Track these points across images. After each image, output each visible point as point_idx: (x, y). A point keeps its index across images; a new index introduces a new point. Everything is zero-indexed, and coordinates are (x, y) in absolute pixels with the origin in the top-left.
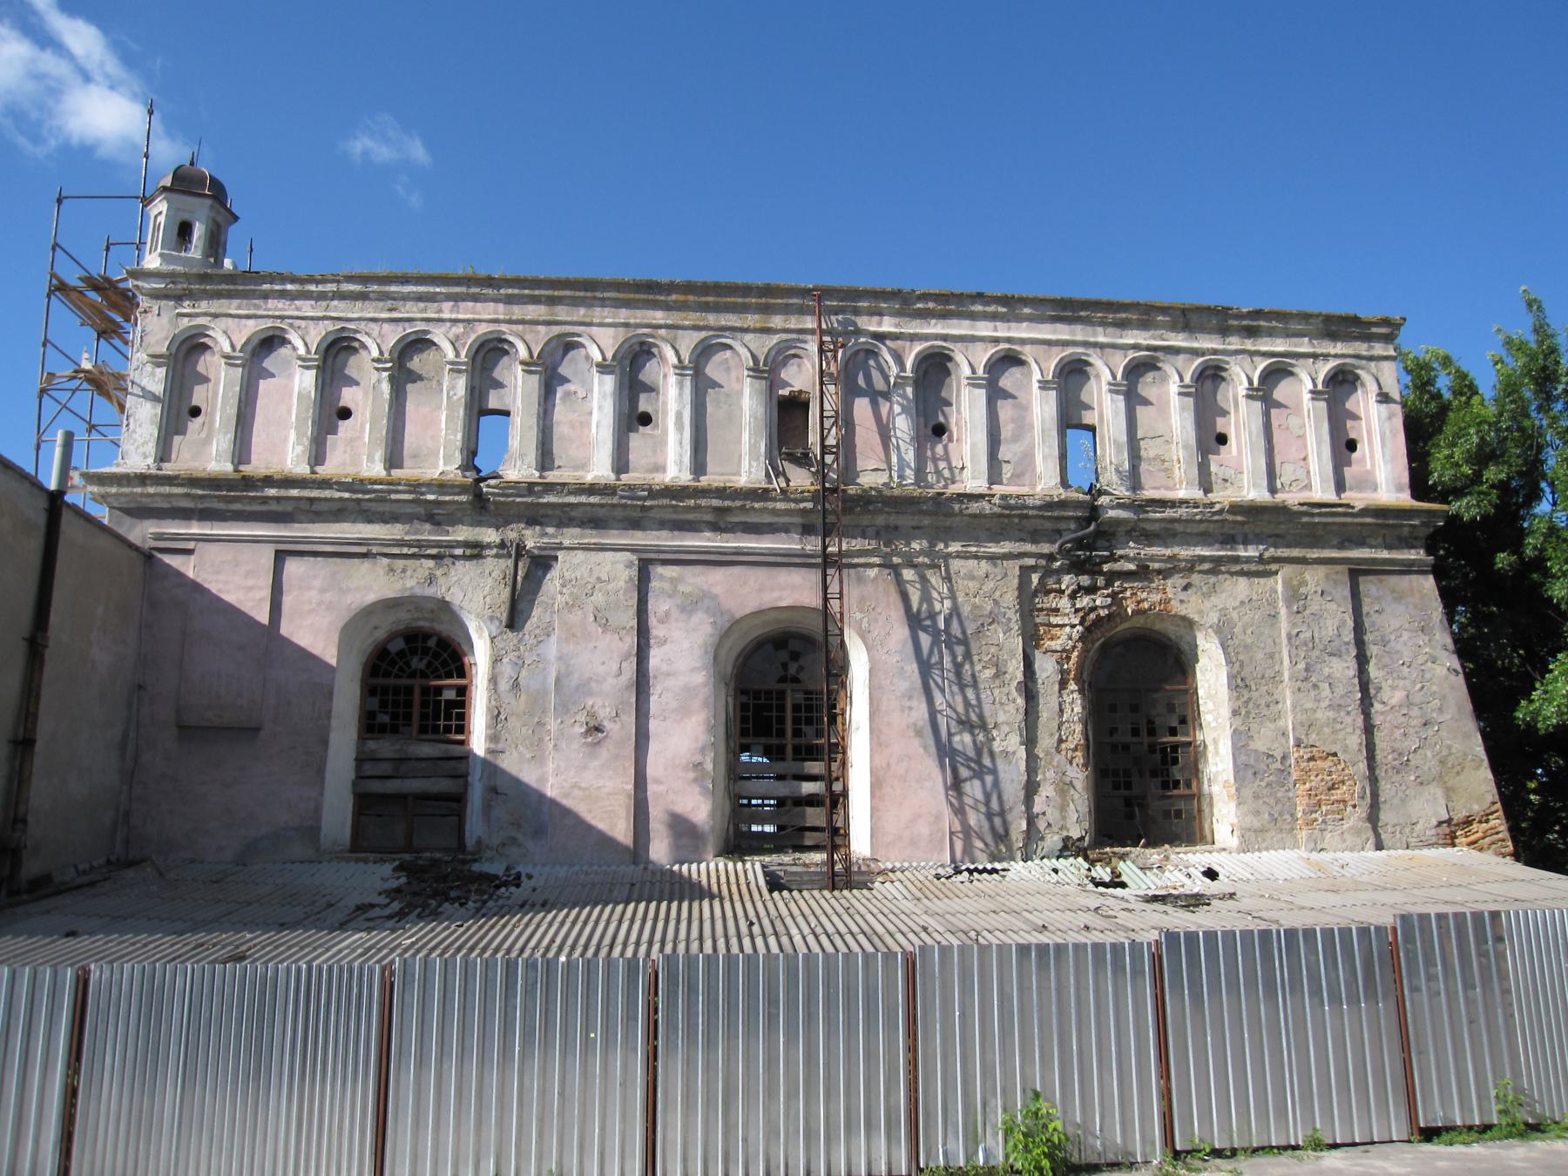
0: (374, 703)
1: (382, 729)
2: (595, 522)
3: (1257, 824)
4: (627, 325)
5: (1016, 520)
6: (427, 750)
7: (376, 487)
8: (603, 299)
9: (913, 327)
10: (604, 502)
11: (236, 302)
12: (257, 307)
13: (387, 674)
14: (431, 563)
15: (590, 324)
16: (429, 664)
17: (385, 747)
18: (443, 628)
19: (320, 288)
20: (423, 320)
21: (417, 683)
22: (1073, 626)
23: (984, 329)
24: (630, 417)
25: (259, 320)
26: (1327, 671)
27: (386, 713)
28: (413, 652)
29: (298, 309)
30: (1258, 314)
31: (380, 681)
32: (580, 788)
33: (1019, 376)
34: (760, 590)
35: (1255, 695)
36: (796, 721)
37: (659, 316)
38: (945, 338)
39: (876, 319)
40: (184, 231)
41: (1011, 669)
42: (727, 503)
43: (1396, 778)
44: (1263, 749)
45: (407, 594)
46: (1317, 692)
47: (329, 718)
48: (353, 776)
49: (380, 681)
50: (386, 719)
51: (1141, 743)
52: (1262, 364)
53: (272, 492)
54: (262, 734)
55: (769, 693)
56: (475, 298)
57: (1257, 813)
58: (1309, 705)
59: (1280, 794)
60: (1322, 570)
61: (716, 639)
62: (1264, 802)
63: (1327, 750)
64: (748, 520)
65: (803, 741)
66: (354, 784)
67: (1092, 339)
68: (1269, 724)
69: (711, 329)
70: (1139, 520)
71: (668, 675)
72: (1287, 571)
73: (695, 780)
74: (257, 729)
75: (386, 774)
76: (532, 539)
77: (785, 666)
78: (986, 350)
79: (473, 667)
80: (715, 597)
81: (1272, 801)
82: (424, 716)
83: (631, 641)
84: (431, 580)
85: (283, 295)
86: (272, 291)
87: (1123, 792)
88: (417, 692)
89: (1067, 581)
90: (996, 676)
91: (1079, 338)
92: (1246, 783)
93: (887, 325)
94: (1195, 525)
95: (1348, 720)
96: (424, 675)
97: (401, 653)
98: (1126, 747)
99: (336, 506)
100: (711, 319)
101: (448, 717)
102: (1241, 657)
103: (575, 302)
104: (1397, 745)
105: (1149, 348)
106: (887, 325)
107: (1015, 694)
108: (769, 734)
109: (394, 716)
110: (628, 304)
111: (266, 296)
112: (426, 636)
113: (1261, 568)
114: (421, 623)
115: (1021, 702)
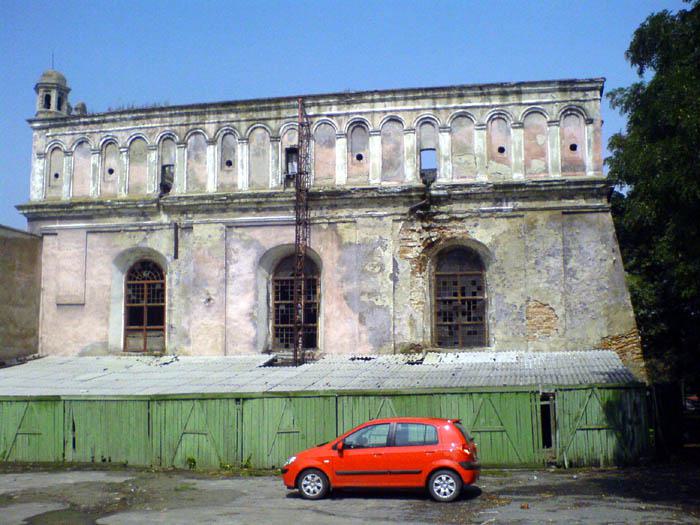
0: (131, 292)
2: (209, 211)
3: (506, 338)
9: (345, 110)
11: (68, 128)
13: (135, 279)
14: (144, 233)
18: (154, 259)
23: (379, 107)
26: (547, 264)
28: (144, 269)
30: (520, 84)
31: (132, 282)
38: (361, 113)
40: (48, 99)
42: (261, 199)
43: (581, 316)
44: (510, 302)
49: (132, 282)
51: (456, 300)
52: (524, 109)
53: (83, 208)
54: (86, 306)
55: (287, 281)
57: (506, 333)
58: (536, 281)
60: (547, 213)
63: (544, 302)
74: (84, 305)
80: (258, 241)
81: (514, 327)
82: (149, 296)
84: (145, 239)
87: (448, 323)
88: (146, 288)
89: (418, 226)
93: (334, 110)
95: (556, 288)
98: (450, 301)
100: (255, 115)
104: (584, 300)
105: (462, 108)
106: (334, 110)
107: (389, 280)
108: (287, 299)
109: (138, 296)
113: (515, 214)
115: (392, 283)
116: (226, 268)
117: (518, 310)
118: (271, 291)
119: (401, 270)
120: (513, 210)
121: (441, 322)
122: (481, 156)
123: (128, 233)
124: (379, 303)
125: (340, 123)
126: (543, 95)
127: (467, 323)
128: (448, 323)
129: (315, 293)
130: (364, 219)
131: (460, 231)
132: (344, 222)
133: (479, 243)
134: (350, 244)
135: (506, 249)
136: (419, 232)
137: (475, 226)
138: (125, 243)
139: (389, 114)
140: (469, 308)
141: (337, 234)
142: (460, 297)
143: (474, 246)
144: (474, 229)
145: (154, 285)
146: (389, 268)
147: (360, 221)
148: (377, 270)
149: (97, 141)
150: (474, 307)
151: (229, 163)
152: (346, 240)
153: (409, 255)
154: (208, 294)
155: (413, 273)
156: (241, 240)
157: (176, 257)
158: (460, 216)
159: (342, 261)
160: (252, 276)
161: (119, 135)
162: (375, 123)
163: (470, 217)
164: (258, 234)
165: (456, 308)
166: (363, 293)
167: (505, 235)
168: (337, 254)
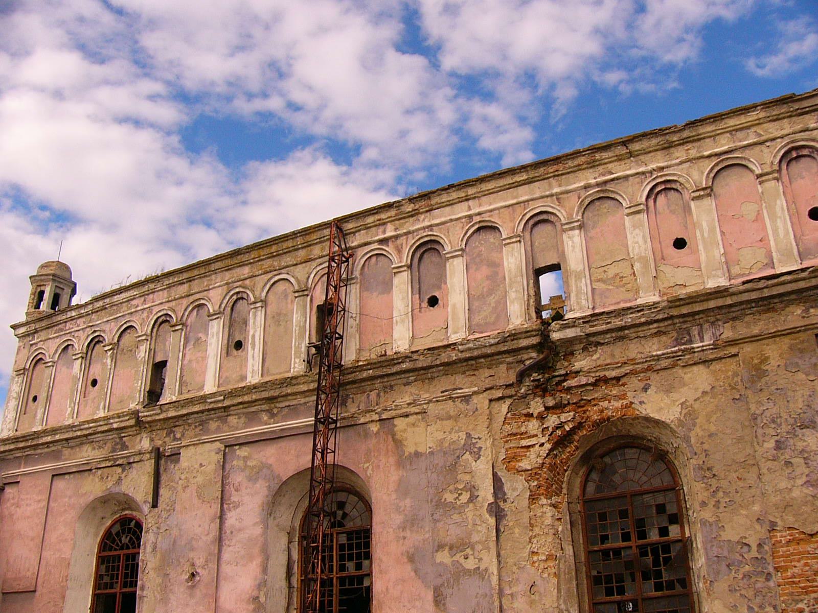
0: (103, 567)
7: (91, 425)
12: (61, 330)
13: (111, 549)
14: (119, 470)
20: (128, 314)
22: (542, 445)
26: (800, 445)
30: (692, 124)
33: (492, 240)
34: (298, 456)
35: (724, 483)
36: (342, 558)
37: (246, 271)
38: (430, 227)
39: (381, 229)
44: (736, 538)
46: (790, 469)
50: (107, 579)
51: (631, 547)
52: (708, 165)
58: (783, 484)
59: (759, 585)
61: (270, 499)
62: (741, 595)
64: (291, 403)
65: (344, 574)
67: (548, 193)
68: (744, 512)
70: (588, 335)
71: (240, 530)
72: (748, 349)
76: (169, 446)
78: (463, 228)
80: (269, 467)
81: (750, 594)
83: (216, 507)
87: (616, 597)
89: (536, 406)
91: (537, 195)
92: (720, 576)
94: (645, 328)
96: (128, 548)
97: (118, 534)
98: (617, 552)
102: (706, 446)
103: (201, 277)
109: (112, 578)
110: (229, 269)
112: (131, 519)
115: (492, 521)
116: (222, 518)
117: (754, 553)
118: (295, 556)
119: (510, 494)
120: (715, 347)
121: (603, 598)
122: (643, 260)
124: (470, 564)
125: (399, 251)
126: (740, 135)
127: (654, 593)
128: (616, 597)
129: (368, 556)
130: (440, 406)
131: (618, 404)
133: (657, 422)
134: (417, 454)
135: (713, 428)
136: (541, 418)
137: (645, 389)
138: (94, 487)
139: (477, 219)
140: (656, 562)
141: (394, 440)
142: (634, 542)
143: (650, 433)
144: (643, 396)
146: (486, 493)
147: (432, 409)
148: (465, 497)
149: (80, 344)
150: (667, 560)
151: (239, 345)
152: (410, 449)
153: (525, 464)
154: (193, 565)
155: (533, 498)
157: (155, 505)
158: (613, 374)
159: (403, 489)
160: (258, 530)
161: (107, 327)
162: (451, 240)
163: (633, 373)
165: (629, 565)
166: (440, 547)
167: (707, 398)
168: (395, 475)
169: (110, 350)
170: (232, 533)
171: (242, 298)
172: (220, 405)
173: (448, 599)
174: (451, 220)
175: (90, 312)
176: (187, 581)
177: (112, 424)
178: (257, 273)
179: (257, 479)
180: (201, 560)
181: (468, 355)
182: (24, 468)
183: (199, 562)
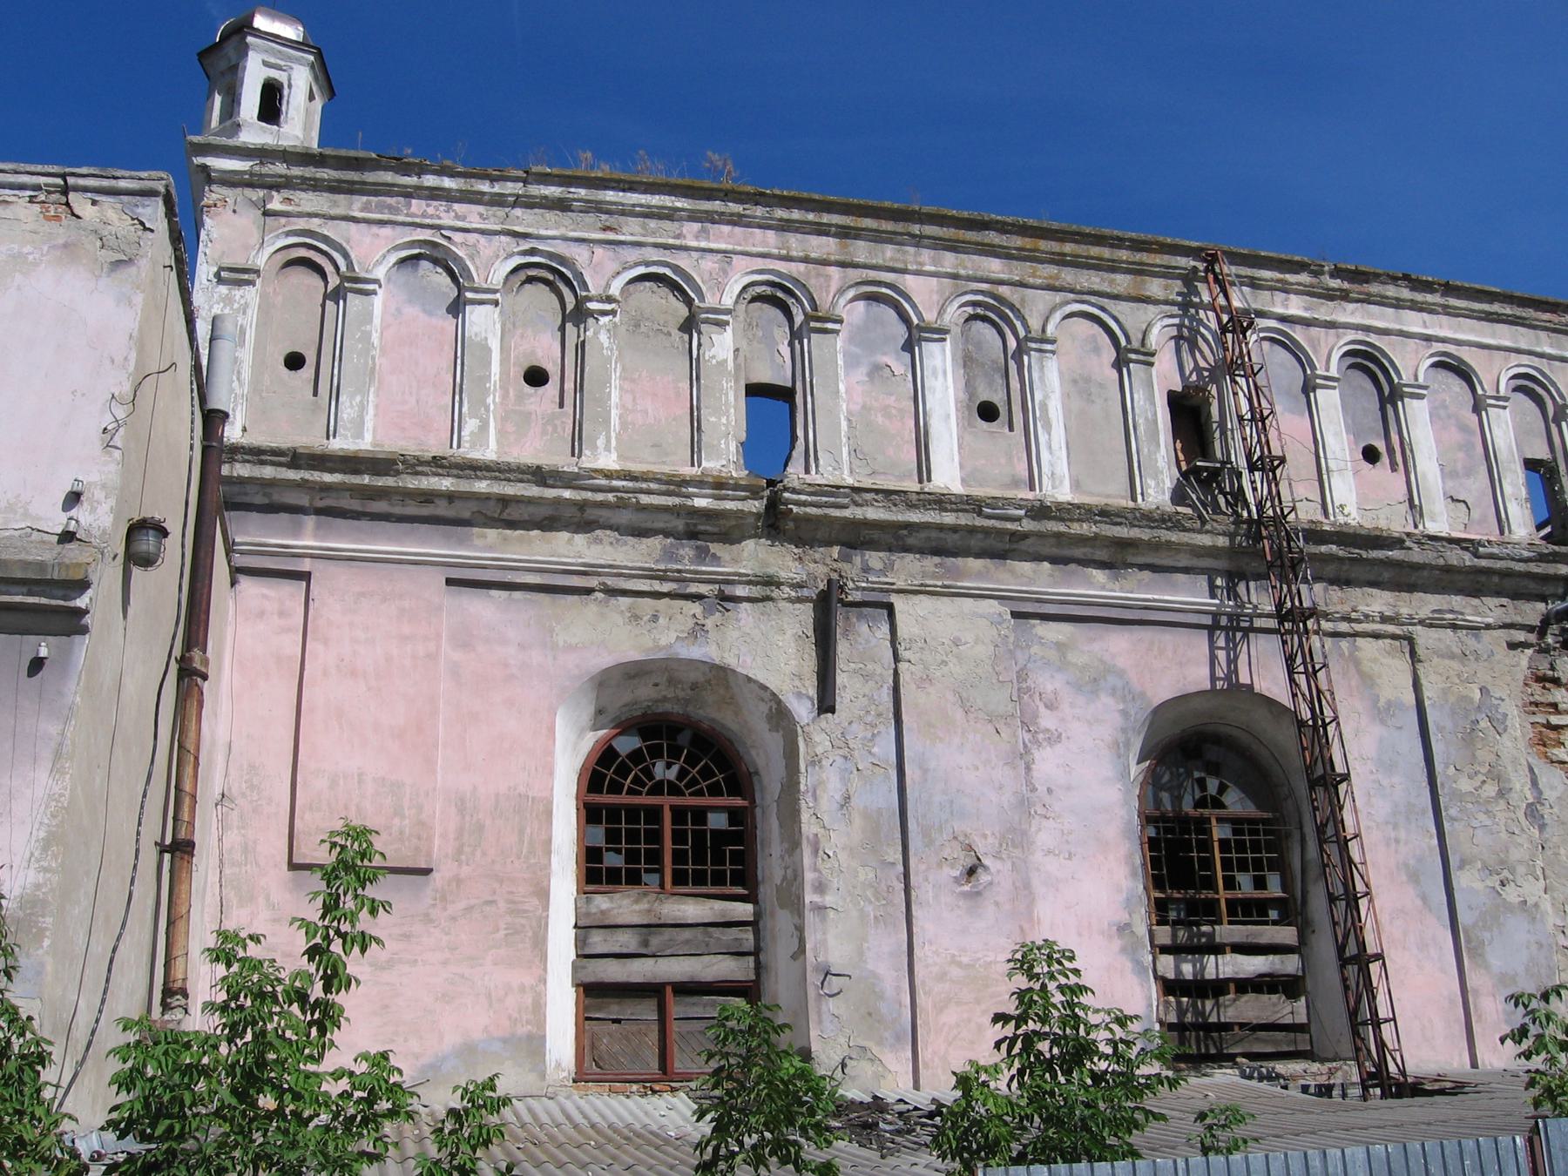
0: (598, 835)
1: (614, 877)
4: (955, 277)
5: (1496, 579)
6: (693, 910)
7: (616, 483)
8: (921, 237)
9: (1325, 311)
10: (963, 522)
12: (393, 209)
13: (615, 788)
14: (696, 608)
15: (904, 271)
16: (682, 774)
17: (624, 905)
19: (497, 188)
20: (656, 245)
21: (666, 801)
24: (968, 407)
25: (399, 229)
27: (618, 851)
28: (656, 753)
29: (457, 217)
32: (960, 965)
36: (1226, 864)
39: (1280, 296)
41: (1518, 786)
45: (660, 655)
47: (549, 853)
48: (573, 957)
50: (613, 860)
54: (434, 874)
56: (736, 221)
66: (575, 967)
69: (1072, 291)
71: (1069, 788)
73: (1123, 950)
75: (625, 951)
77: (1202, 784)
79: (755, 779)
80: (1121, 674)
82: (679, 857)
84: (697, 631)
85: (435, 194)
86: (419, 188)
88: (667, 816)
90: (1501, 794)
91: (1523, 346)
96: (674, 790)
97: (636, 756)
99: (544, 512)
101: (719, 859)
103: (878, 237)
109: (632, 857)
110: (953, 246)
111: (408, 194)
114: (668, 707)
123: (624, 601)
132: (1376, 636)
141: (1361, 673)
145: (700, 815)
148: (1491, 790)
154: (970, 848)
156: (1063, 665)
157: (826, 704)
164: (1118, 645)
169: (604, 313)
170: (1050, 791)
171: (984, 319)
172: (1009, 526)
173: (1488, 949)
174: (1402, 334)
175: (511, 199)
176: (956, 880)
177: (688, 496)
178: (1031, 280)
179: (1095, 693)
180: (990, 840)
181: (1484, 563)
182: (316, 537)
183: (981, 847)
